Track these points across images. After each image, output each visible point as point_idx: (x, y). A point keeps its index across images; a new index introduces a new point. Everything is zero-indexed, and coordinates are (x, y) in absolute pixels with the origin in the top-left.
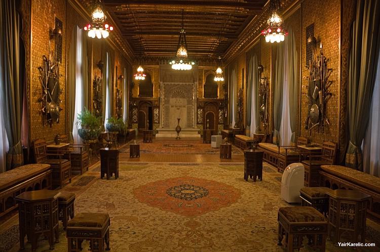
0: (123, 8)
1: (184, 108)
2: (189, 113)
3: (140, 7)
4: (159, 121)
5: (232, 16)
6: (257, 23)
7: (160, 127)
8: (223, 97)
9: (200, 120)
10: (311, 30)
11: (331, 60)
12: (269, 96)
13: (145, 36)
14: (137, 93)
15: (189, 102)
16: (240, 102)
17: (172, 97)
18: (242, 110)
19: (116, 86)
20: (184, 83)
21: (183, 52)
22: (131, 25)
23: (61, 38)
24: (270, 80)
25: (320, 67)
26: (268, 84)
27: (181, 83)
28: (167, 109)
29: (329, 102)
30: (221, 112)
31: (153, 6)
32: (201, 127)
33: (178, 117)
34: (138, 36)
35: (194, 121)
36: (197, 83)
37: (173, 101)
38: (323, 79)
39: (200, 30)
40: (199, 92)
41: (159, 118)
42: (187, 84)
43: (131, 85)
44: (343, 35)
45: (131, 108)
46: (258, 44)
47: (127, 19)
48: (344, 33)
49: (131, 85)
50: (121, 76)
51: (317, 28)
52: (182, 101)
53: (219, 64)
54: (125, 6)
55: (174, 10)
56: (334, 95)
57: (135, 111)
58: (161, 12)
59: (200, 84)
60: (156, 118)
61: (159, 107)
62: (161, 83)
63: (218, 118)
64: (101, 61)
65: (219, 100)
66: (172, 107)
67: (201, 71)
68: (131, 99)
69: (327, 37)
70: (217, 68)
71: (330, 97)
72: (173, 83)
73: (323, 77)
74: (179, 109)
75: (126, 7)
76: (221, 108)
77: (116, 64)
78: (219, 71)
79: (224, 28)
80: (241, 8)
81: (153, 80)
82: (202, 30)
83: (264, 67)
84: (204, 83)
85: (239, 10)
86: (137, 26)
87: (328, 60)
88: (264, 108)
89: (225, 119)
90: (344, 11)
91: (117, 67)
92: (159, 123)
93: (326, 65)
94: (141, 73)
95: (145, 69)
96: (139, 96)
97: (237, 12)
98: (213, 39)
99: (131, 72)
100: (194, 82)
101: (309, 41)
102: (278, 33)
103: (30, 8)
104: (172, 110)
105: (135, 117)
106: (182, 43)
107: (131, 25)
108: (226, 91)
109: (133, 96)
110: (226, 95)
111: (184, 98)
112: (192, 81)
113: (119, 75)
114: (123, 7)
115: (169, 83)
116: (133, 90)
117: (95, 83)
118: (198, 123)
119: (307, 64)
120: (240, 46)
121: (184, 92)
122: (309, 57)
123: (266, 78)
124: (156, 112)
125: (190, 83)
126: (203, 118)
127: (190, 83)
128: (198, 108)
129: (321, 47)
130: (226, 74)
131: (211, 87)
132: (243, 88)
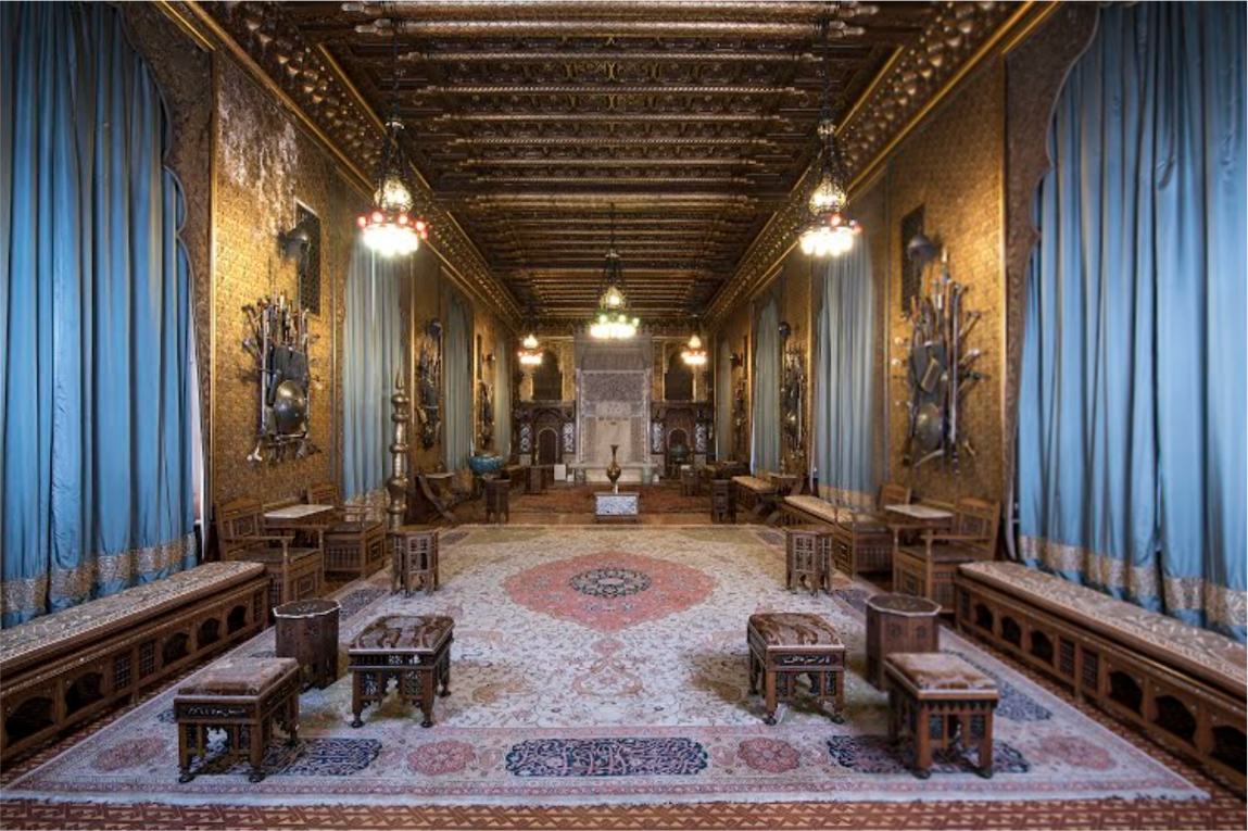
0: (481, 202)
1: (623, 422)
2: (636, 433)
3: (519, 200)
4: (574, 449)
5: (720, 219)
6: (776, 231)
7: (578, 460)
8: (703, 399)
9: (658, 445)
10: (912, 223)
11: (974, 288)
12: (805, 391)
13: (540, 271)
14: (528, 392)
15: (635, 408)
16: (740, 407)
17: (602, 400)
18: (744, 424)
19: (479, 376)
20: (624, 372)
21: (614, 298)
22: (505, 246)
23: (313, 252)
24: (808, 355)
25: (942, 311)
26: (802, 362)
27: (619, 372)
28: (591, 423)
29: (972, 397)
30: (700, 430)
31: (546, 197)
32: (660, 459)
33: (613, 439)
34: (524, 273)
35: (646, 448)
36: (649, 371)
37: (604, 408)
38: (951, 339)
39: (653, 256)
40: (650, 386)
41: (574, 442)
42: (631, 372)
43: (516, 376)
44: (1012, 220)
45: (516, 426)
46: (779, 278)
47: (495, 231)
48: (1013, 213)
49: (516, 376)
50: (489, 358)
51: (931, 216)
52: (620, 408)
53: (695, 328)
54: (484, 197)
55: (594, 205)
56: (988, 378)
57: (526, 430)
58: (565, 213)
59: (658, 372)
60: (568, 442)
61: (574, 421)
62: (578, 370)
63: (693, 441)
64: (433, 321)
65: (697, 404)
66: (601, 419)
67: (658, 345)
68: (515, 402)
69: (959, 232)
70: (690, 336)
71: (974, 384)
72: (601, 372)
73: (951, 333)
74: (614, 423)
75: (488, 201)
76: (700, 422)
77: (477, 331)
78: (695, 342)
79: (705, 249)
80: (740, 197)
81: (561, 367)
82: (658, 255)
83: (793, 326)
84: (665, 370)
85: (736, 201)
86: (519, 249)
87: (966, 289)
88: (793, 418)
89: (710, 443)
90: (1012, 160)
91: (479, 338)
92: (574, 453)
93: (960, 305)
94: (534, 351)
95: (543, 344)
96: (534, 397)
97: (733, 208)
98: (681, 272)
99: (514, 347)
100: (644, 368)
101: (914, 244)
102: (833, 229)
103: (210, 170)
104: (600, 426)
105: (525, 441)
106: (613, 273)
107: (505, 246)
108: (711, 386)
109: (522, 399)
110: (711, 395)
111: (623, 399)
112: (641, 365)
113: (485, 353)
114: (482, 201)
115: (595, 372)
116: (521, 388)
117: (420, 368)
118: (653, 453)
119: (906, 307)
120: (740, 288)
121: (619, 391)
122: (911, 286)
123: (799, 352)
124: (568, 429)
125: (638, 372)
126: (664, 439)
127: (638, 372)
128: (653, 421)
129: (944, 259)
130: (713, 348)
131: (678, 378)
132: (746, 377)
